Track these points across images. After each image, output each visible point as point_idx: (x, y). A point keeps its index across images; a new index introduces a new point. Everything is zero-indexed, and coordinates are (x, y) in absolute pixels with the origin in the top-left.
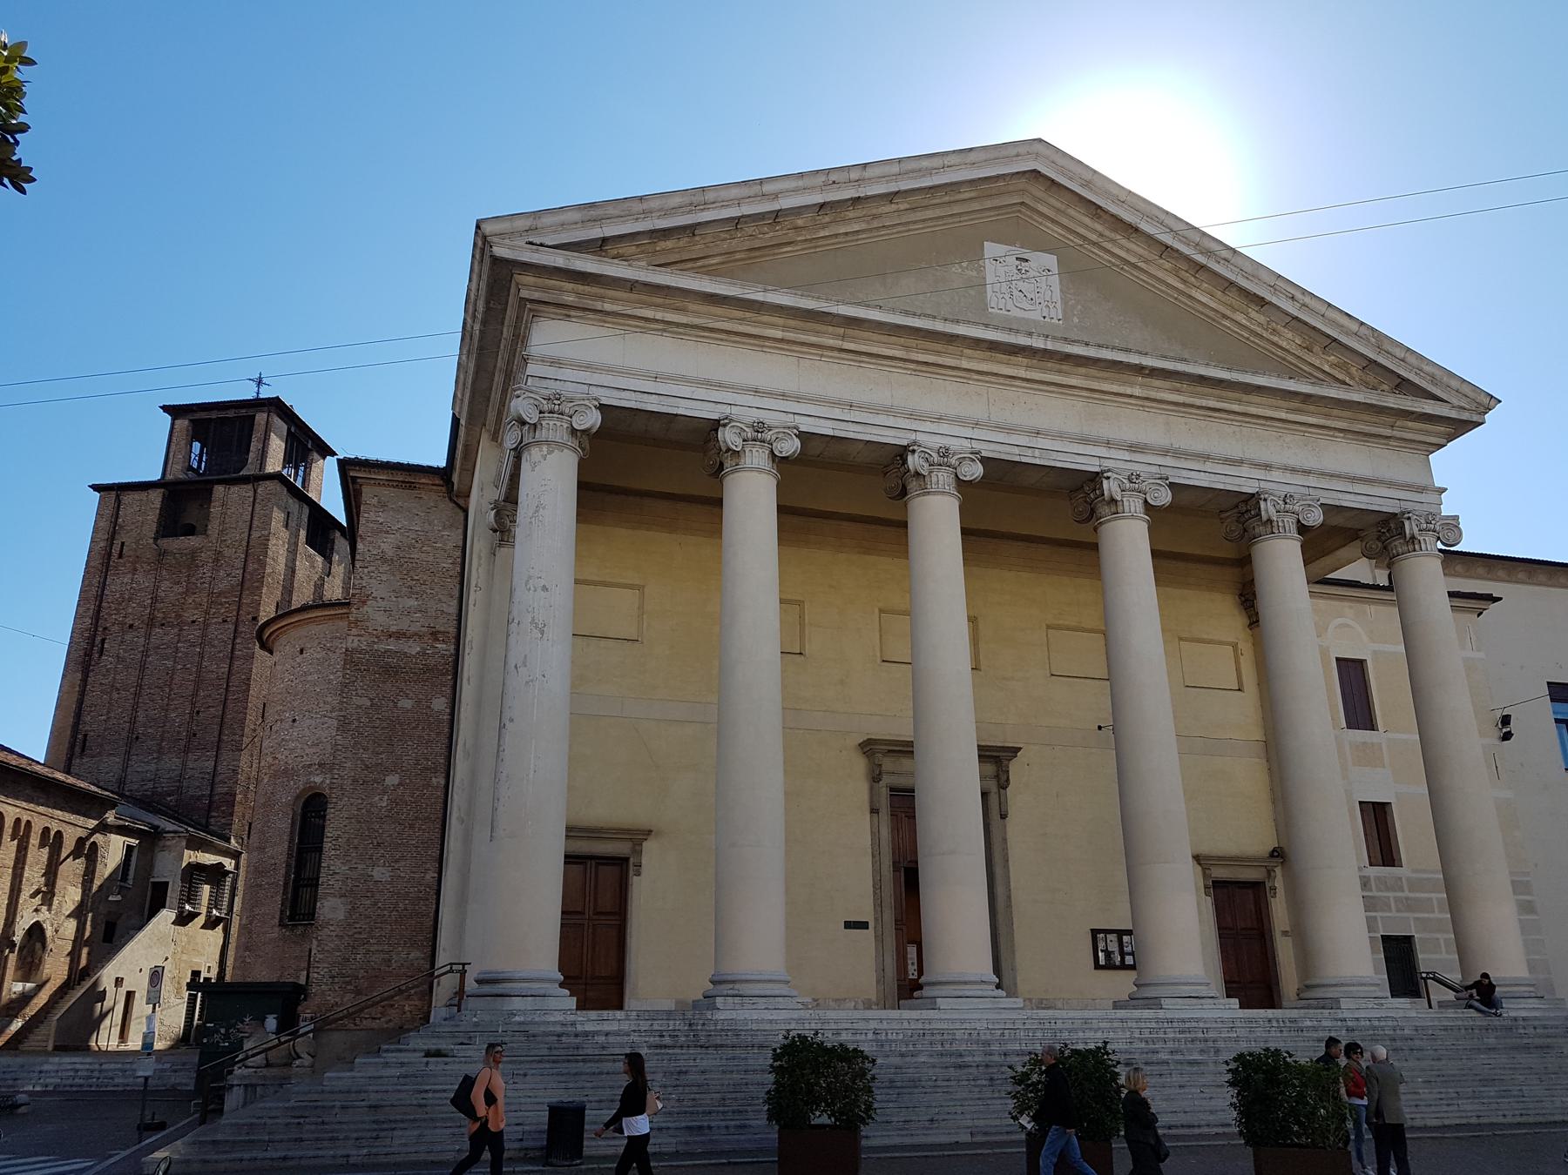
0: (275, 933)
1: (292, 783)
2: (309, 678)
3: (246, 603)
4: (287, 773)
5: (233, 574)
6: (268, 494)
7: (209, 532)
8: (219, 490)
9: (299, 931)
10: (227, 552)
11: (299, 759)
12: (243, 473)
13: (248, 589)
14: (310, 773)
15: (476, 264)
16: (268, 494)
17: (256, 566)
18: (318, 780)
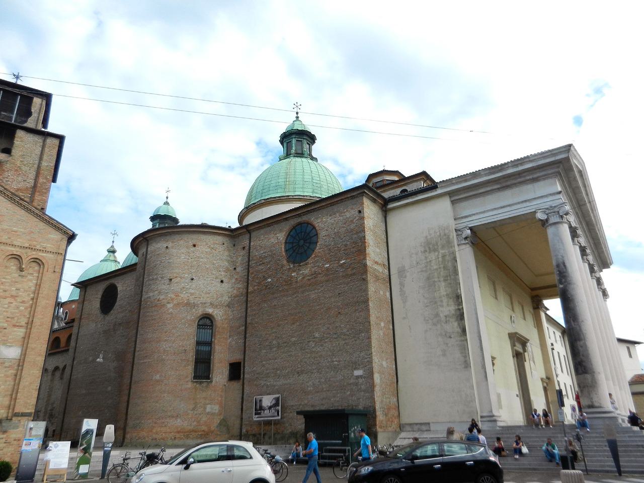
0: (190, 385)
1: (194, 310)
2: (201, 260)
3: (37, 199)
4: (189, 305)
5: (28, 181)
6: (53, 145)
7: (12, 154)
8: (20, 134)
9: (204, 385)
10: (24, 168)
11: (197, 299)
12: (25, 125)
13: (39, 192)
14: (205, 307)
15: (549, 153)
16: (53, 145)
17: (45, 181)
18: (210, 311)
